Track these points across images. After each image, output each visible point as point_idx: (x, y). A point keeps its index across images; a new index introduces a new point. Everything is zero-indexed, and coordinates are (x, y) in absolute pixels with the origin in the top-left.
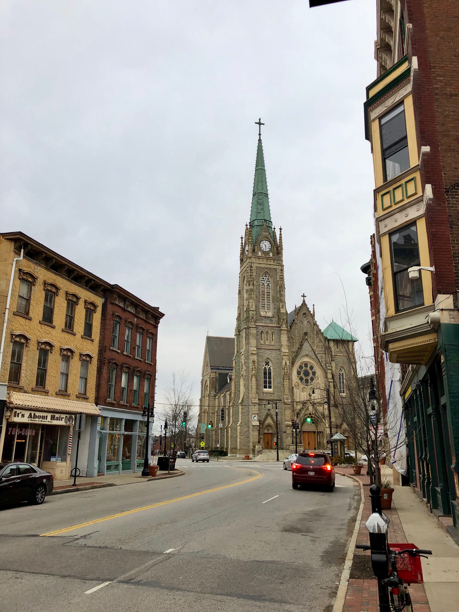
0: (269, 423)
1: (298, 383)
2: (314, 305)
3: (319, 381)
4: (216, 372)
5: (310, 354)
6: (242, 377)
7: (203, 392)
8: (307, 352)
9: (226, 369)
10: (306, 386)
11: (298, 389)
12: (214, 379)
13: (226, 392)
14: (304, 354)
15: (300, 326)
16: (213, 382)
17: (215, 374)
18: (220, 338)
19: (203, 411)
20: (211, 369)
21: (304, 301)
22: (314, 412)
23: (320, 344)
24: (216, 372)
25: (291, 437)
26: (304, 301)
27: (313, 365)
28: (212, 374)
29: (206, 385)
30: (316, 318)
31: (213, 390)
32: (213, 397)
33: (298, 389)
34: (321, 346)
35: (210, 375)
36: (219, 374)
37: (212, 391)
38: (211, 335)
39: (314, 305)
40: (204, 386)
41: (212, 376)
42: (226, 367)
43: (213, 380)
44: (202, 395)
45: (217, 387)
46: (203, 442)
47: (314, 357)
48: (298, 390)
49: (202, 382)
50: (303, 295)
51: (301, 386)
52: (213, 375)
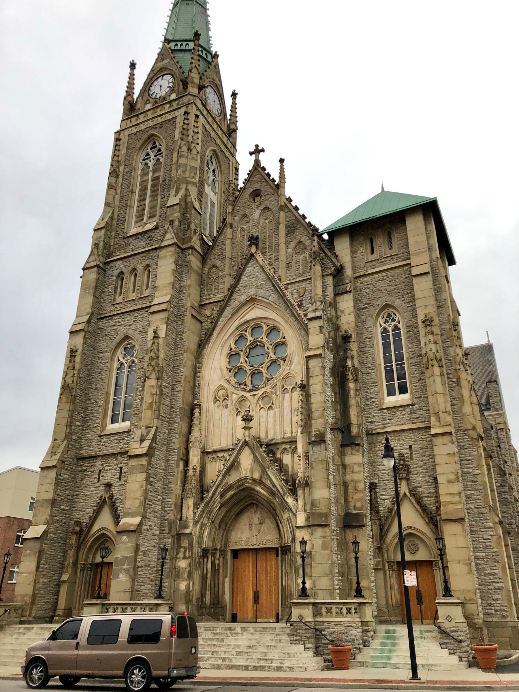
0: (103, 528)
1: (224, 389)
2: (282, 161)
3: (292, 368)
5: (261, 292)
8: (252, 292)
10: (247, 395)
11: (226, 406)
14: (243, 298)
15: (242, 230)
21: (257, 162)
22: (256, 476)
23: (301, 257)
25: (127, 571)
26: (257, 162)
27: (277, 324)
30: (289, 191)
33: (226, 406)
34: (305, 260)
39: (282, 161)
47: (274, 297)
48: (225, 411)
50: (260, 148)
51: (234, 396)
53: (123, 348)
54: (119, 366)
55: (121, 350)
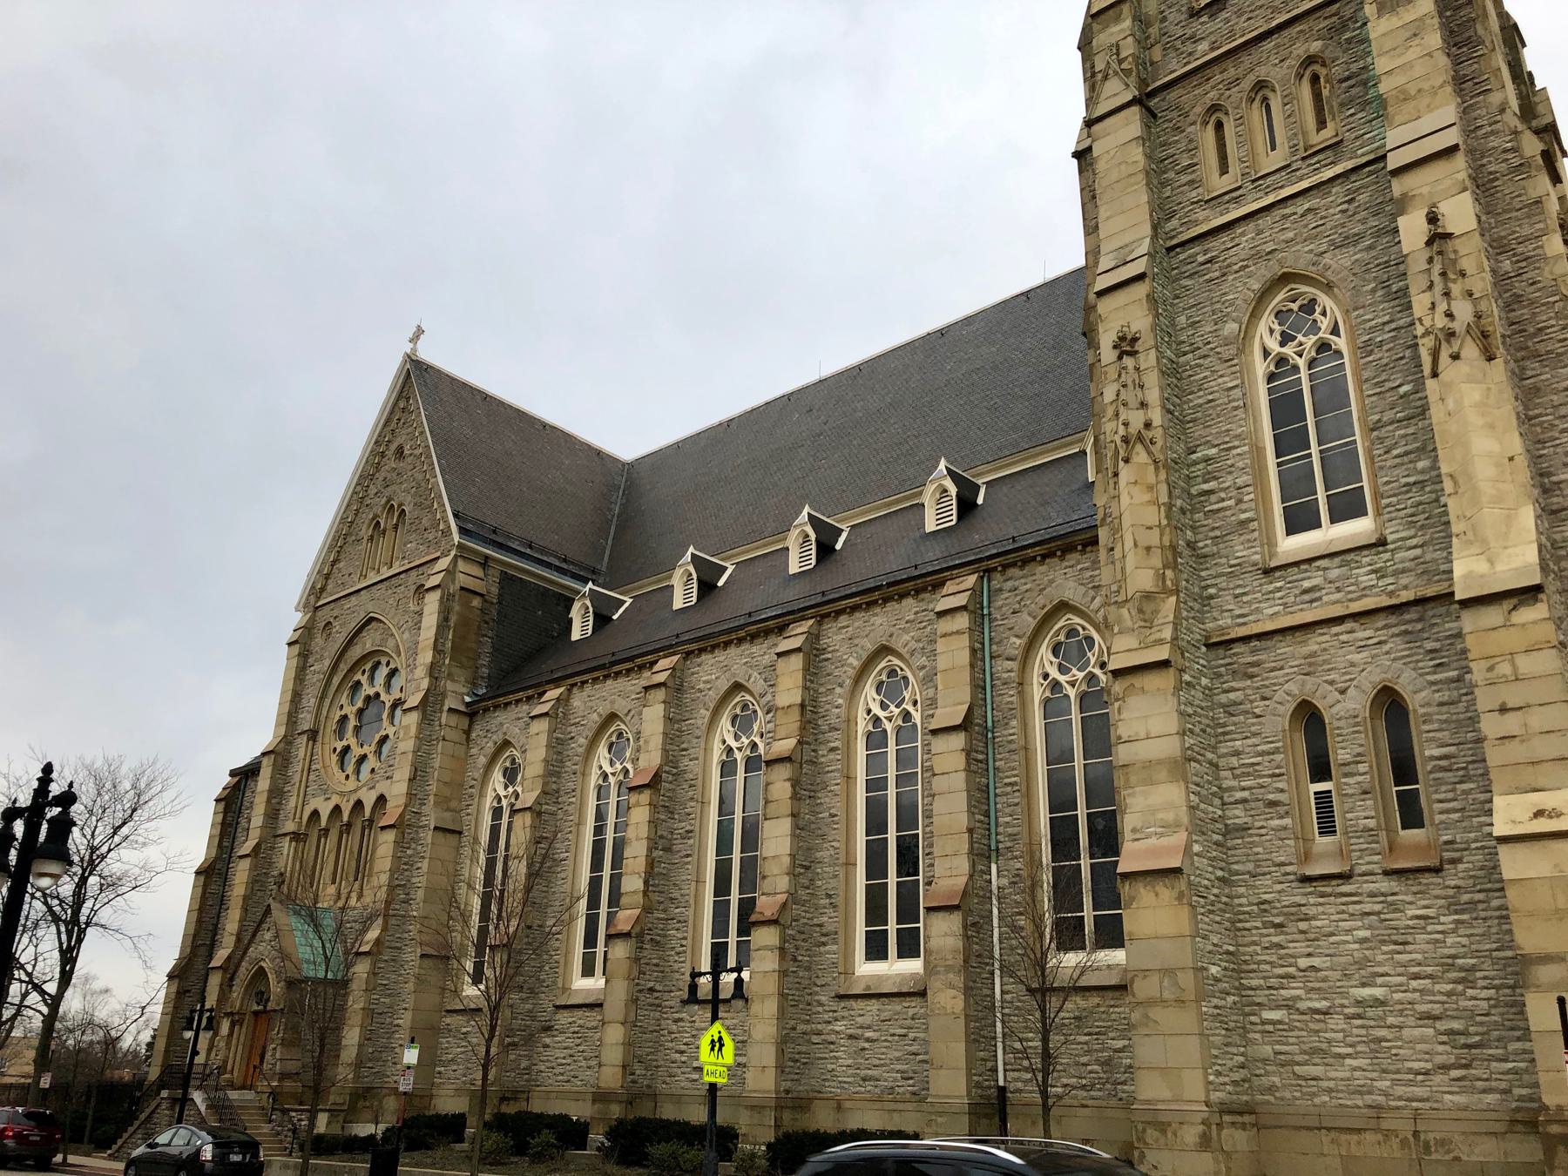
4: (485, 562)
6: (1471, 351)
7: (310, 701)
9: (548, 565)
12: (476, 602)
13: (688, 654)
16: (464, 622)
17: (478, 572)
18: (486, 398)
19: (290, 826)
20: (463, 531)
24: (485, 562)
28: (461, 565)
29: (356, 652)
31: (462, 675)
32: (454, 720)
35: (450, 572)
36: (507, 580)
37: (450, 676)
38: (429, 353)
40: (319, 667)
41: (462, 580)
42: (542, 550)
43: (466, 605)
44: (291, 717)
45: (484, 660)
46: (716, 1030)
49: (302, 643)
52: (469, 574)
53: (1272, 317)
54: (1272, 368)
55: (1267, 321)
